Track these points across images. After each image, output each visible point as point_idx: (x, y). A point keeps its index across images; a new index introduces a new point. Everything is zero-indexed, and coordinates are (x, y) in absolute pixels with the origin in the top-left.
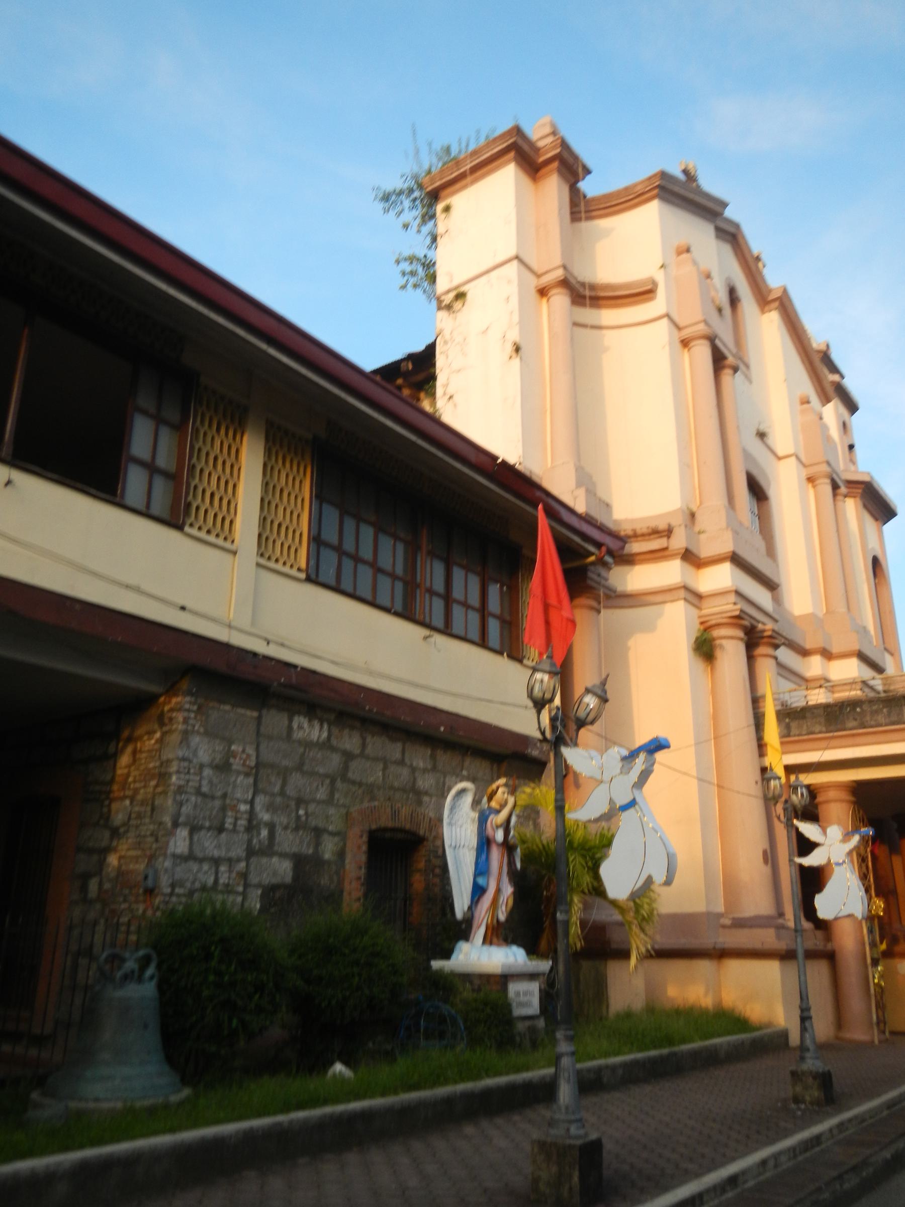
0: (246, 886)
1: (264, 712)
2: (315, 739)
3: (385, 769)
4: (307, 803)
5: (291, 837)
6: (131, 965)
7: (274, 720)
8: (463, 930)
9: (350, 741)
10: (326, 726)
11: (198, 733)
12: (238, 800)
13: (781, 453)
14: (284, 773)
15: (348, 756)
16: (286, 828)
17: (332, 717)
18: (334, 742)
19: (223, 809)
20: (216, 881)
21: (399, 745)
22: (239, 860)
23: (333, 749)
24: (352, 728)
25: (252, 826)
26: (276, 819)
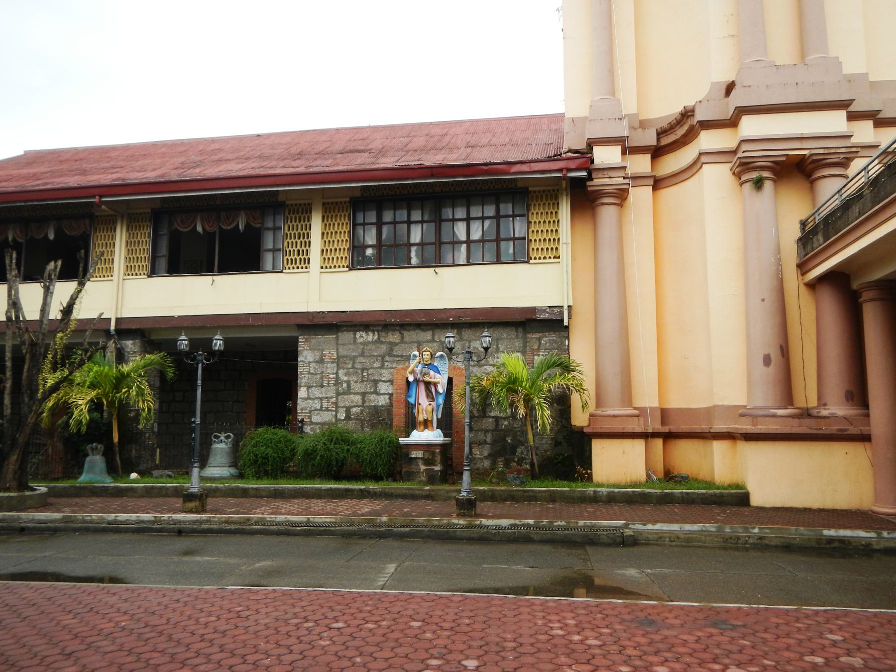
0: (337, 407)
1: (340, 334)
2: (371, 340)
4: (367, 369)
5: (360, 385)
6: (222, 438)
7: (346, 336)
9: (394, 337)
10: (376, 333)
11: (307, 350)
12: (329, 373)
14: (353, 359)
15: (392, 345)
16: (356, 382)
17: (380, 328)
18: (383, 339)
19: (322, 378)
20: (321, 407)
21: (430, 332)
22: (332, 397)
23: (382, 343)
24: (394, 330)
25: (338, 382)
26: (350, 379)
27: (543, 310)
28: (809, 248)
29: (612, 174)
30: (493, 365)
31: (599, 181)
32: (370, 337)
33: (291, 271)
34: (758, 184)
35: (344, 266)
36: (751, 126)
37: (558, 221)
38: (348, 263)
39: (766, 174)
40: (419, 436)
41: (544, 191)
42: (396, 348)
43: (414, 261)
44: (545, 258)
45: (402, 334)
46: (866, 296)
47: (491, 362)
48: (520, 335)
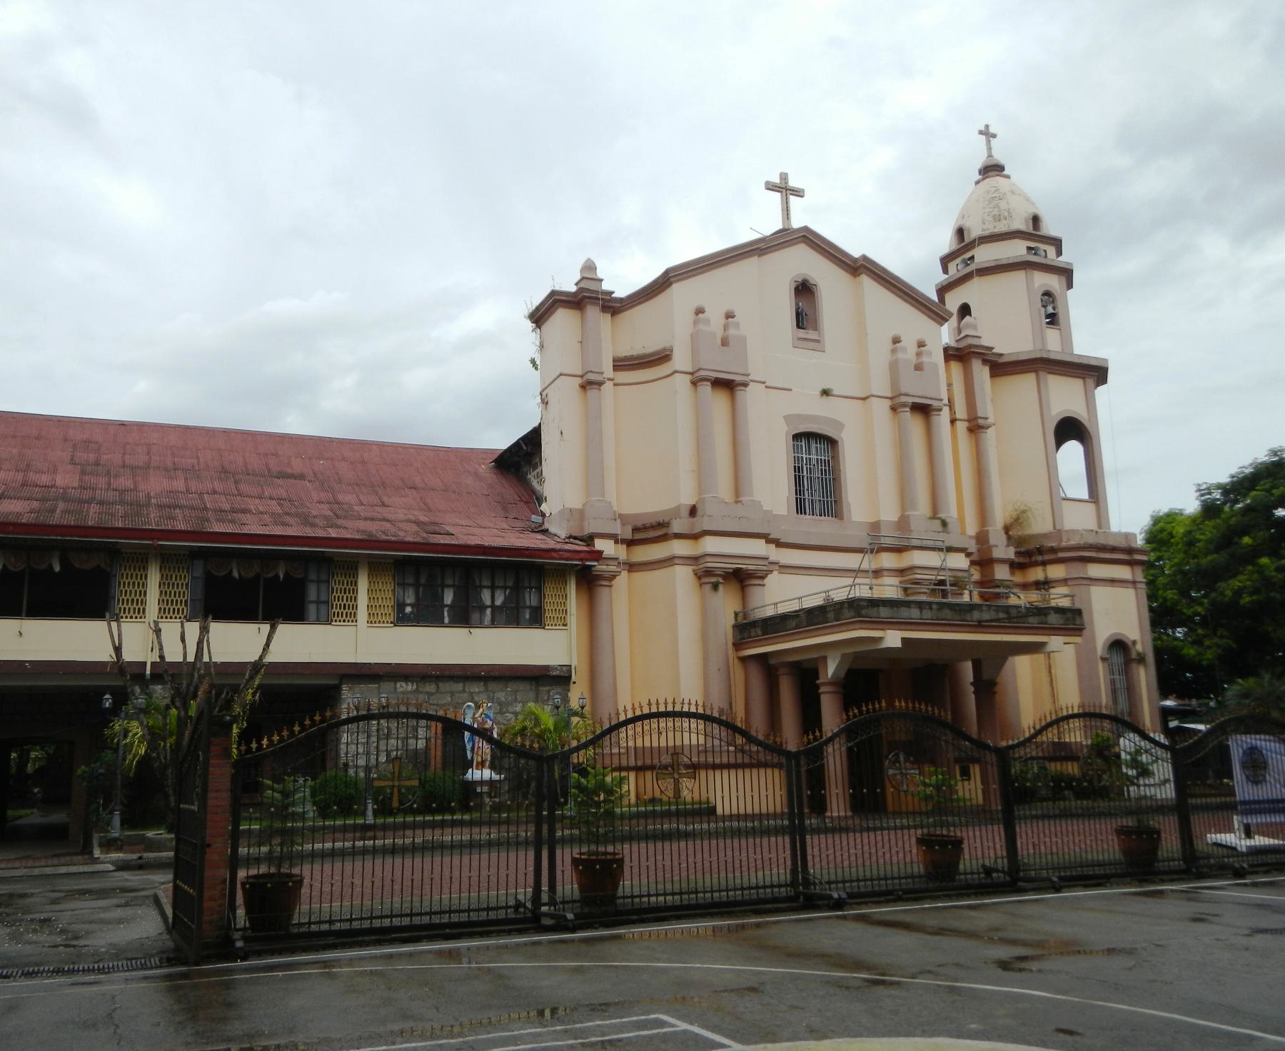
3: (451, 697)
7: (387, 686)
8: (468, 765)
9: (431, 688)
13: (864, 396)
15: (430, 694)
17: (418, 679)
18: (420, 689)
21: (461, 684)
24: (431, 681)
27: (554, 668)
28: (746, 635)
29: (609, 562)
30: (513, 713)
31: (599, 567)
32: (410, 687)
33: (338, 623)
34: (715, 587)
35: (387, 622)
36: (711, 545)
37: (566, 595)
38: (392, 620)
39: (721, 580)
40: (475, 774)
41: (555, 570)
42: (432, 697)
43: (446, 620)
44: (556, 625)
45: (438, 685)
46: (782, 671)
47: (511, 710)
48: (533, 688)
